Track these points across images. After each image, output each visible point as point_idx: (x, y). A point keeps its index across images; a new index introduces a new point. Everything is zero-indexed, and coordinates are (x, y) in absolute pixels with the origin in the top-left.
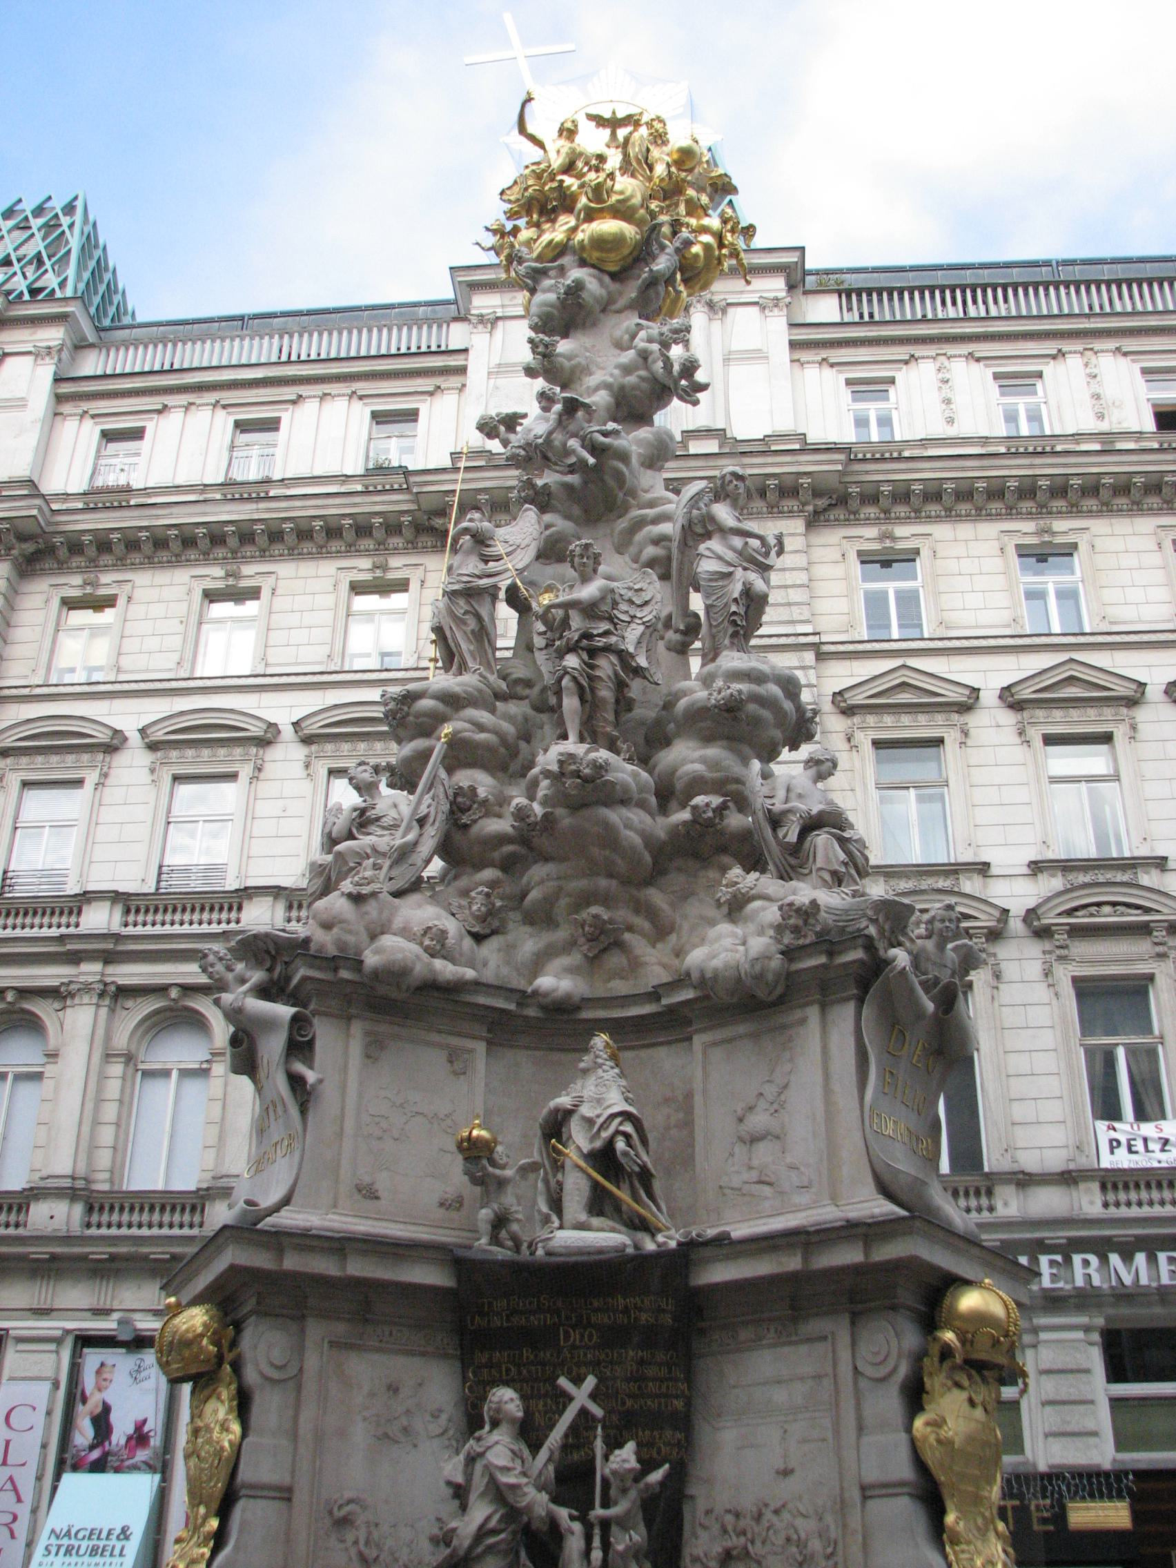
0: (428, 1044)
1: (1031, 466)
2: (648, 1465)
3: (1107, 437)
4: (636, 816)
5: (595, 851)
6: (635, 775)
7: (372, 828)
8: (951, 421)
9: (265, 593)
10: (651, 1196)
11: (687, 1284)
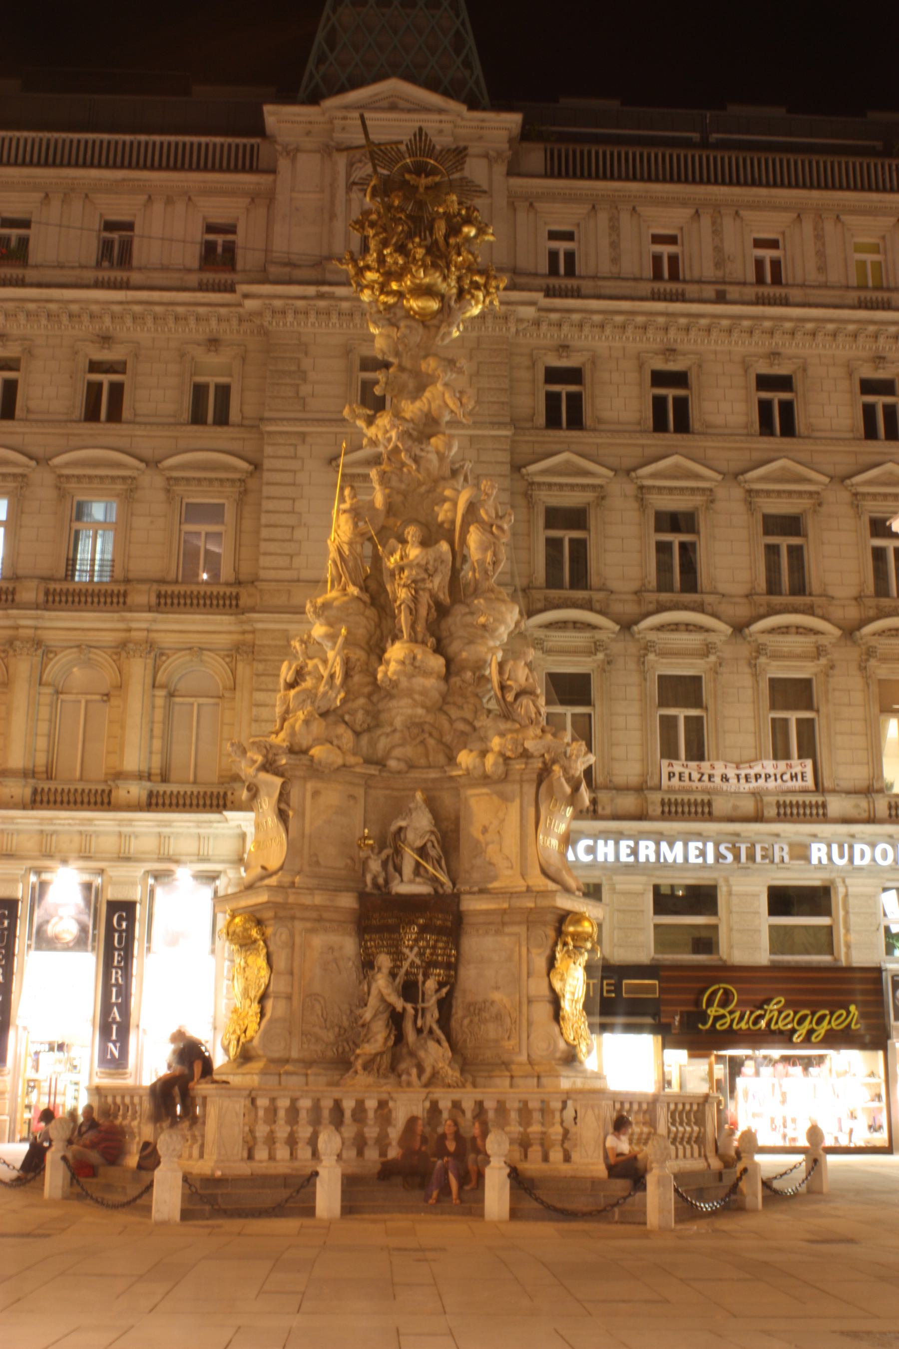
2: (441, 985)
5: (417, 697)
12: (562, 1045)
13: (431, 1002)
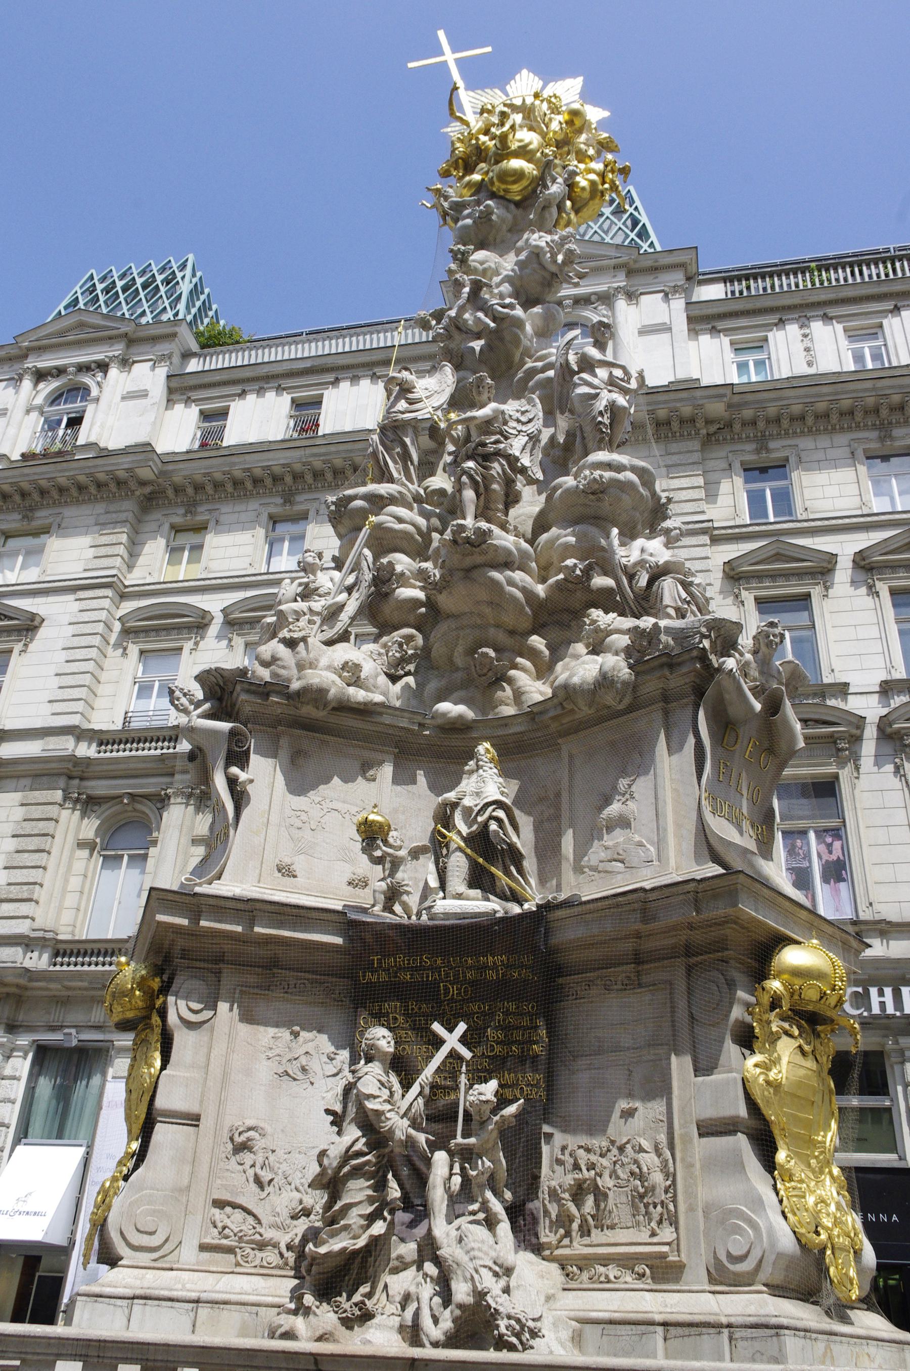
6: (516, 544)
8: (810, 364)
10: (520, 871)
12: (787, 1242)
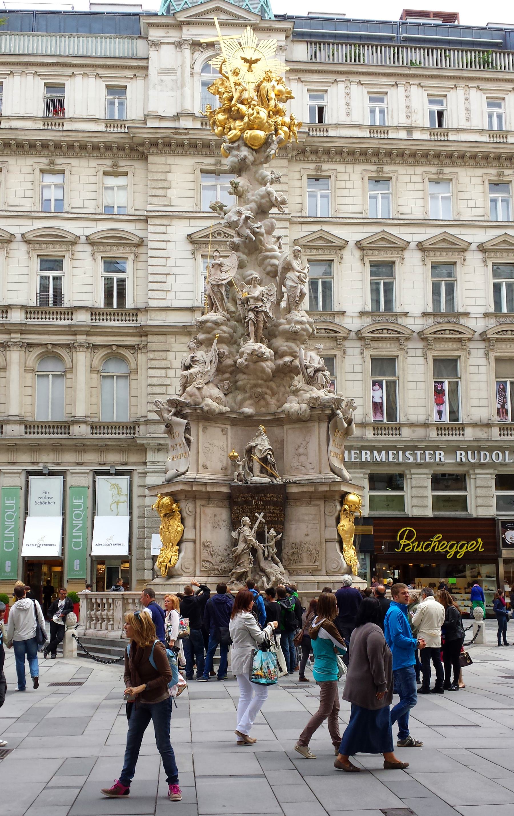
0: (218, 427)
1: (379, 143)
3: (410, 130)
4: (270, 364)
5: (259, 374)
7: (197, 363)
8: (348, 114)
9: (67, 173)
11: (285, 490)
12: (345, 565)
13: (272, 543)
